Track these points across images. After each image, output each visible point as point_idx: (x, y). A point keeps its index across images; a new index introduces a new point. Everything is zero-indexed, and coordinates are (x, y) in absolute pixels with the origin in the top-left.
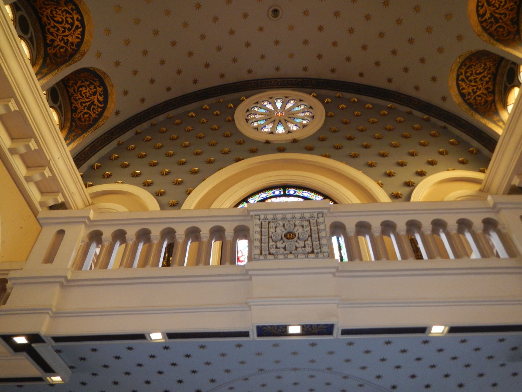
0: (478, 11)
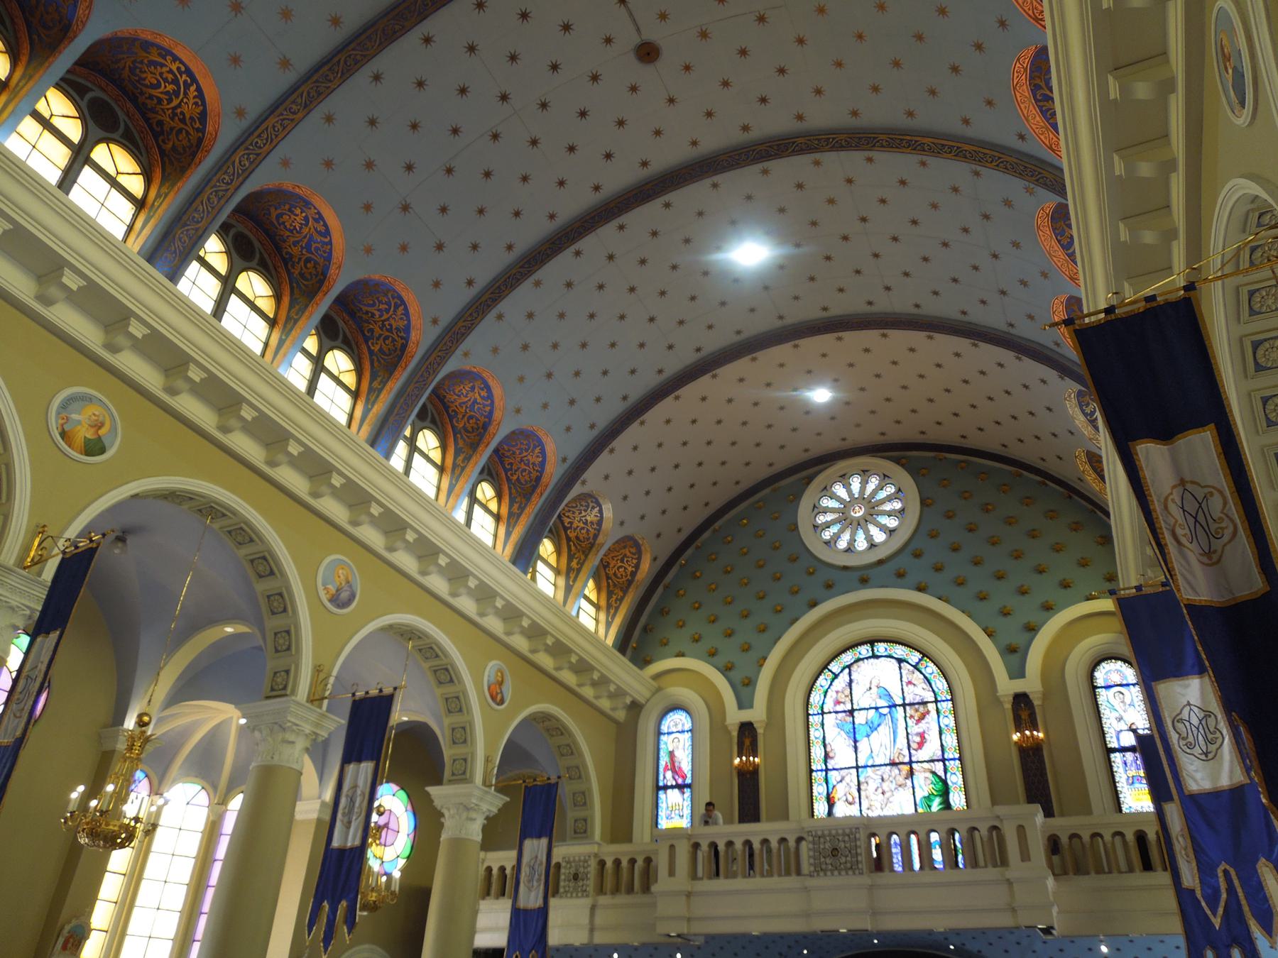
0: (1083, 411)
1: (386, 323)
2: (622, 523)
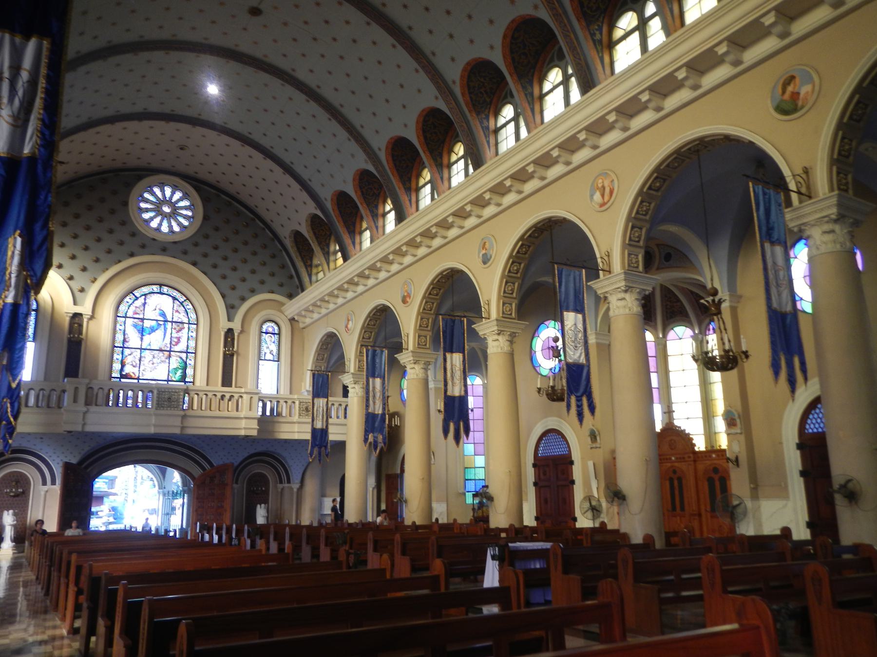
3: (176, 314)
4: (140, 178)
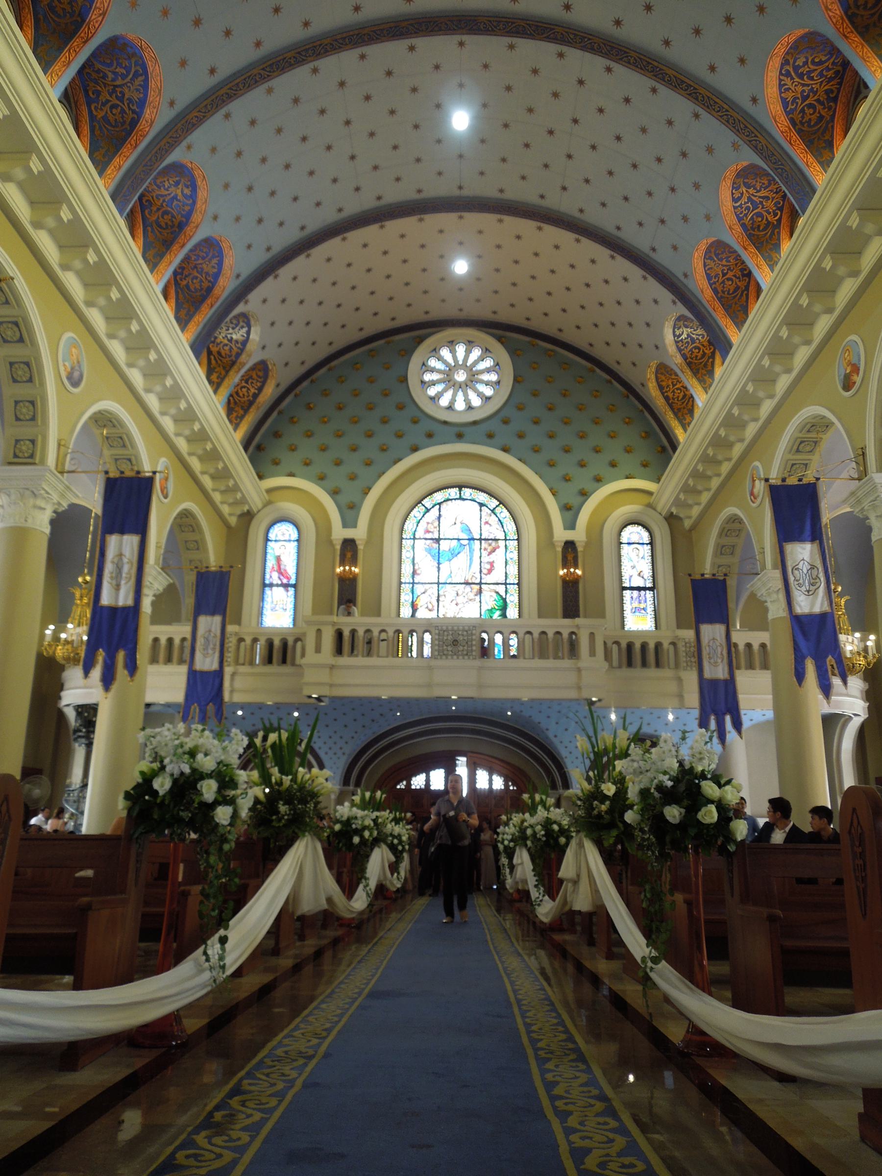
0: (674, 332)
1: (119, 90)
2: (264, 348)
3: (485, 528)
4: (420, 340)
